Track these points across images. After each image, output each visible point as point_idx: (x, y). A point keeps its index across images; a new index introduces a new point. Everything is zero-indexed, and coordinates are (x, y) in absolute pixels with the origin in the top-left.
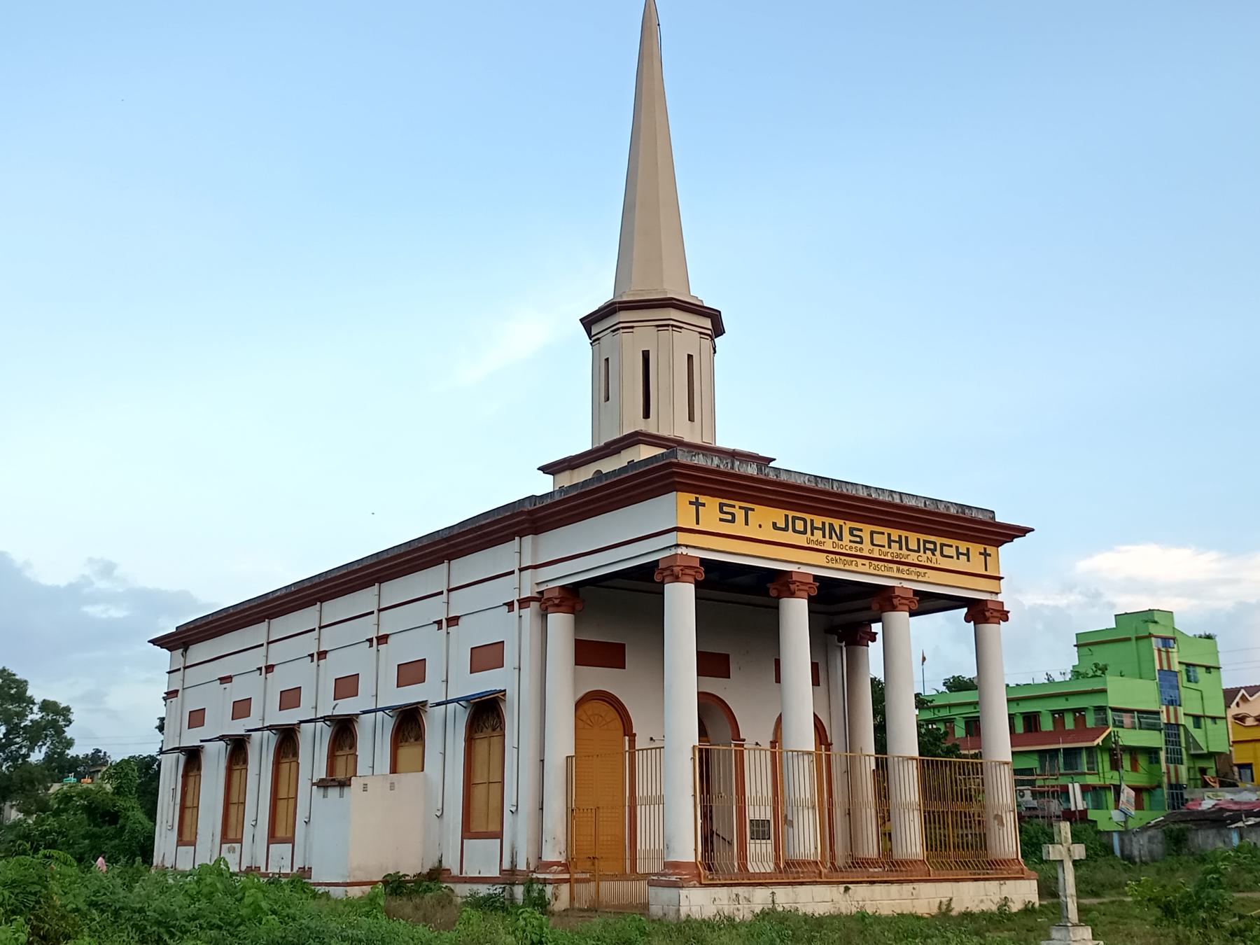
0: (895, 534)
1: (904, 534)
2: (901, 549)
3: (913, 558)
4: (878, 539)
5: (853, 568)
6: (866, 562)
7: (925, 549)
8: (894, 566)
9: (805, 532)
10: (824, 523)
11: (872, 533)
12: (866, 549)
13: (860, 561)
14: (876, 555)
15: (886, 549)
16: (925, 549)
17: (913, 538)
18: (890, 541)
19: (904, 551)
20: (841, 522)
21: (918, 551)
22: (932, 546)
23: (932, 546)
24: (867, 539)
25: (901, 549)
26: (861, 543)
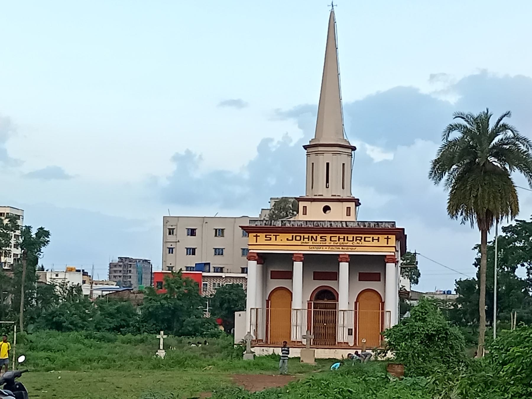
0: (342, 236)
1: (346, 236)
2: (344, 241)
3: (350, 244)
4: (333, 239)
6: (328, 247)
7: (356, 240)
8: (341, 247)
9: (300, 240)
10: (309, 236)
11: (331, 237)
12: (328, 242)
13: (324, 247)
14: (332, 244)
16: (356, 240)
17: (350, 237)
18: (339, 239)
19: (346, 241)
20: (317, 235)
21: (353, 240)
22: (360, 238)
23: (360, 238)
24: (328, 239)
25: (344, 241)
26: (326, 241)
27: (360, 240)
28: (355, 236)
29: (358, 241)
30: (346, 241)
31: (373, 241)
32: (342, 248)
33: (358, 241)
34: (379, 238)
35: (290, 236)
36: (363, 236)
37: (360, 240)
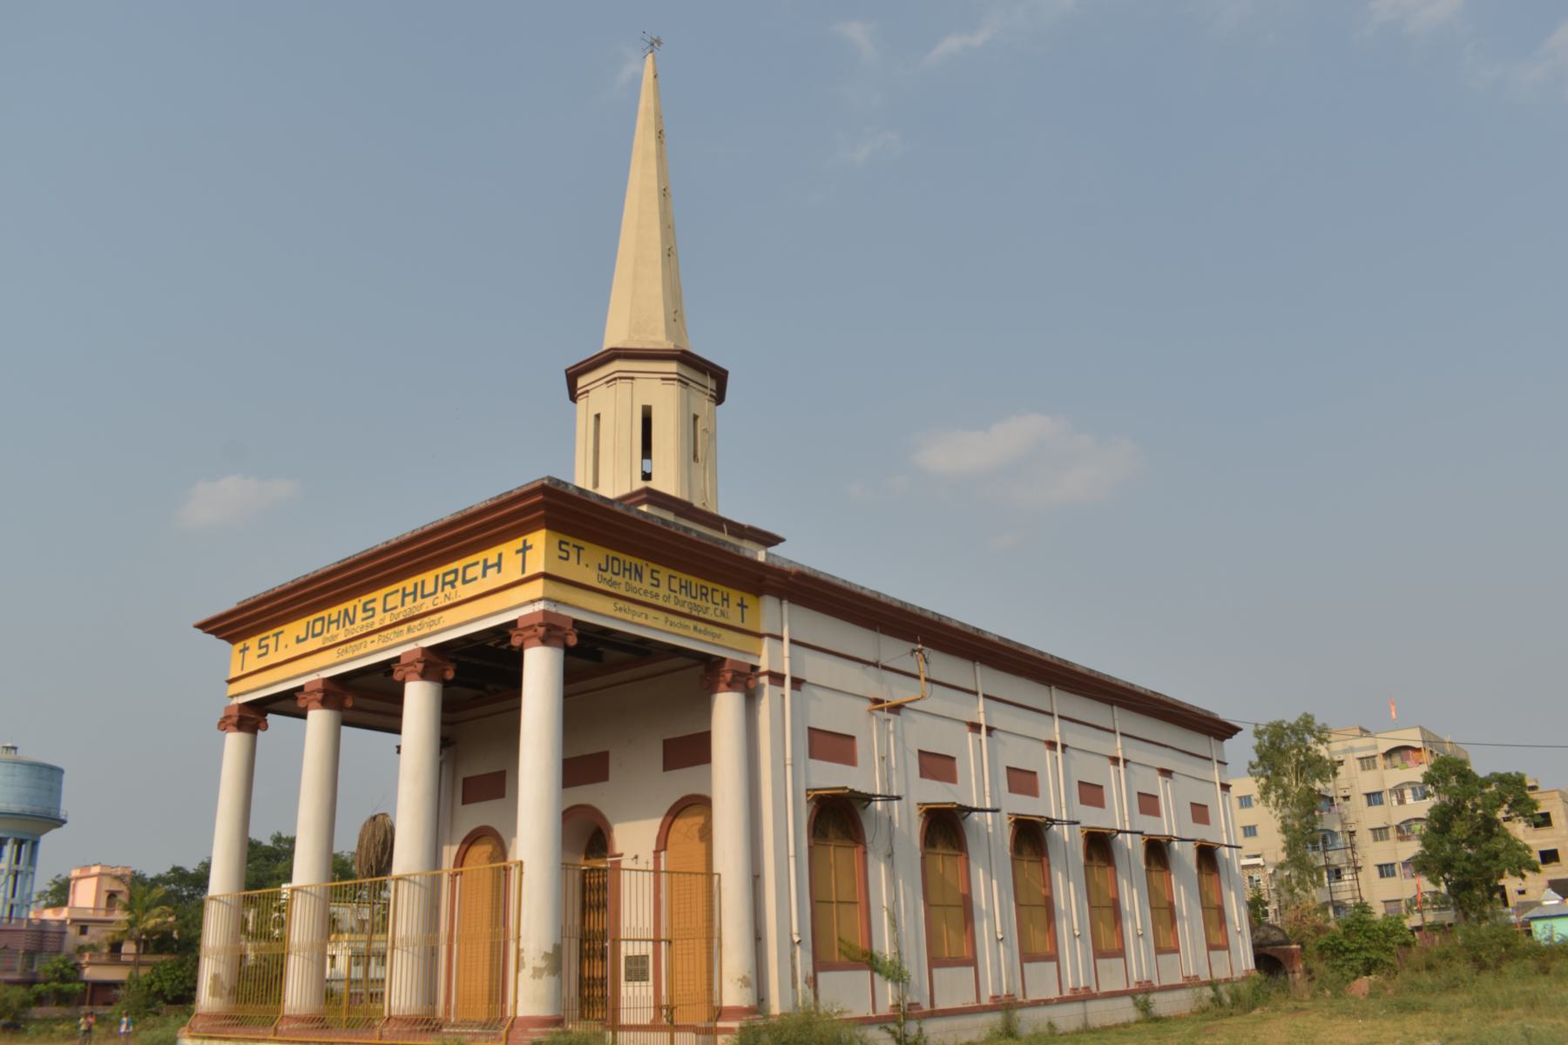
0: (408, 584)
3: (428, 604)
5: (362, 651)
6: (375, 637)
7: (444, 584)
8: (404, 627)
15: (400, 609)
17: (429, 577)
27: (452, 583)
28: (440, 571)
29: (448, 588)
30: (419, 600)
31: (484, 575)
32: (409, 630)
33: (448, 588)
34: (500, 555)
35: (297, 627)
36: (458, 565)
37: (452, 583)
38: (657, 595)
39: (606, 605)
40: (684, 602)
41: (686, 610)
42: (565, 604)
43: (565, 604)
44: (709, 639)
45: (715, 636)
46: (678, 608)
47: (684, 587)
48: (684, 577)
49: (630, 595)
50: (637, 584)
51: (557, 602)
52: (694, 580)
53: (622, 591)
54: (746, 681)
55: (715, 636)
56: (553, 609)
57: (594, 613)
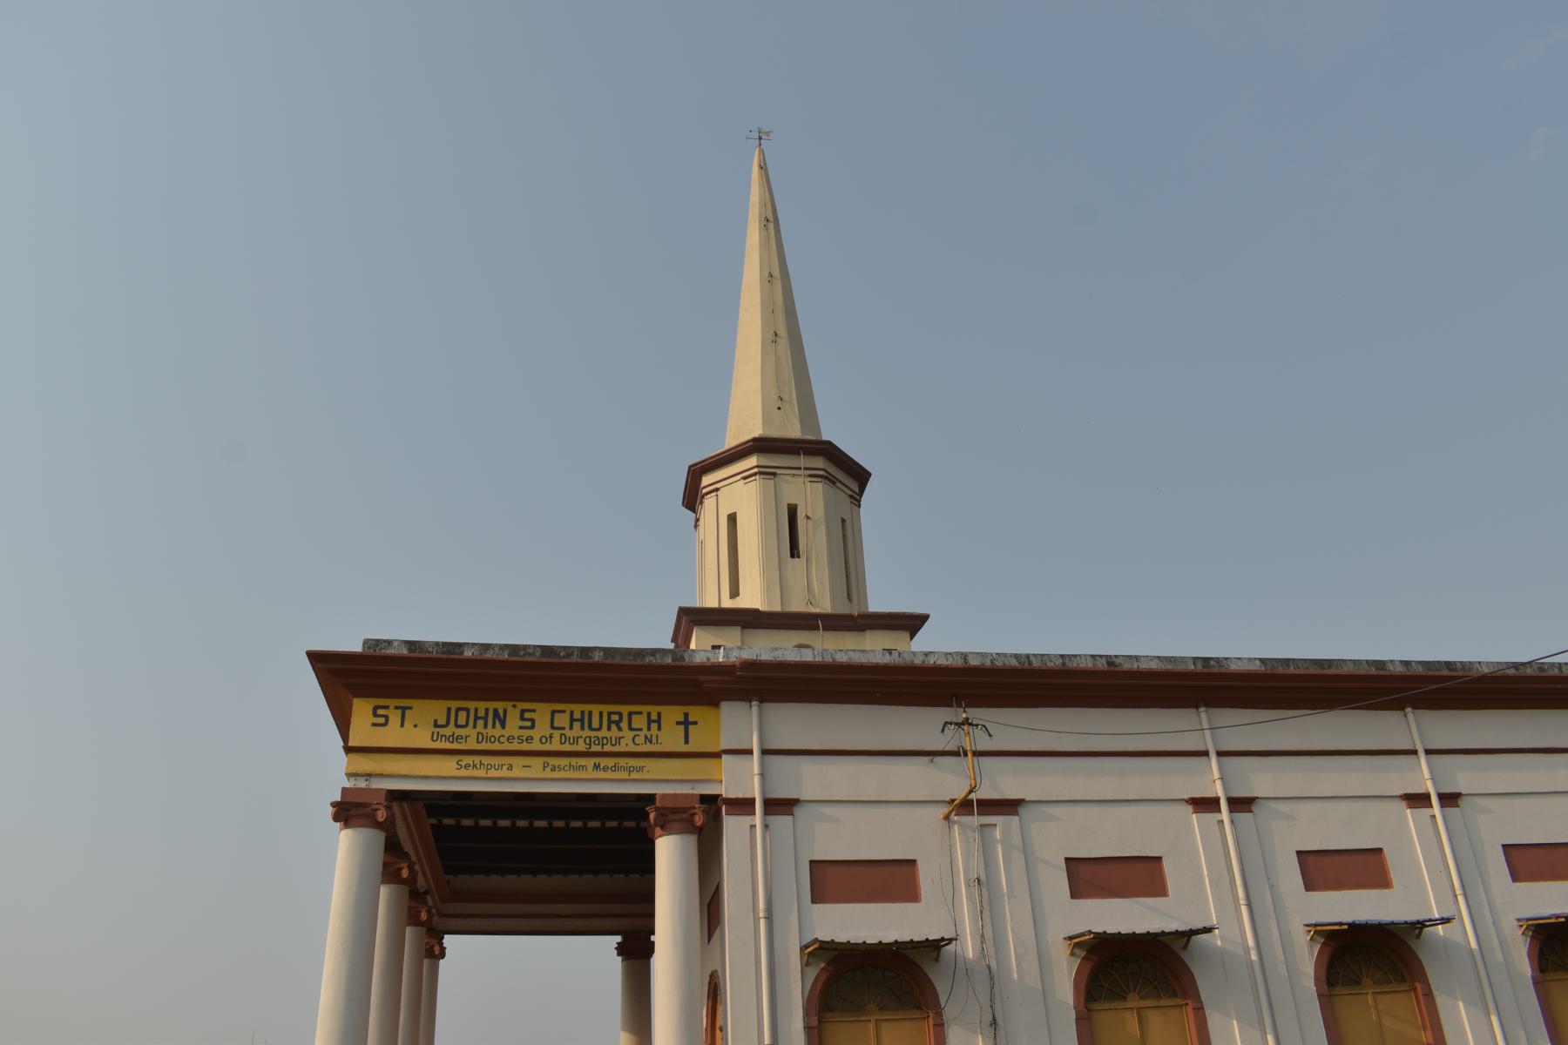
38: (529, 739)
39: (447, 766)
40: (580, 737)
41: (581, 747)
42: (381, 775)
43: (381, 775)
44: (624, 775)
45: (630, 770)
46: (567, 747)
47: (583, 721)
48: (577, 708)
49: (483, 746)
50: (498, 731)
51: (368, 776)
52: (596, 709)
53: (472, 744)
54: (704, 820)
55: (630, 770)
56: (362, 784)
57: (425, 777)
